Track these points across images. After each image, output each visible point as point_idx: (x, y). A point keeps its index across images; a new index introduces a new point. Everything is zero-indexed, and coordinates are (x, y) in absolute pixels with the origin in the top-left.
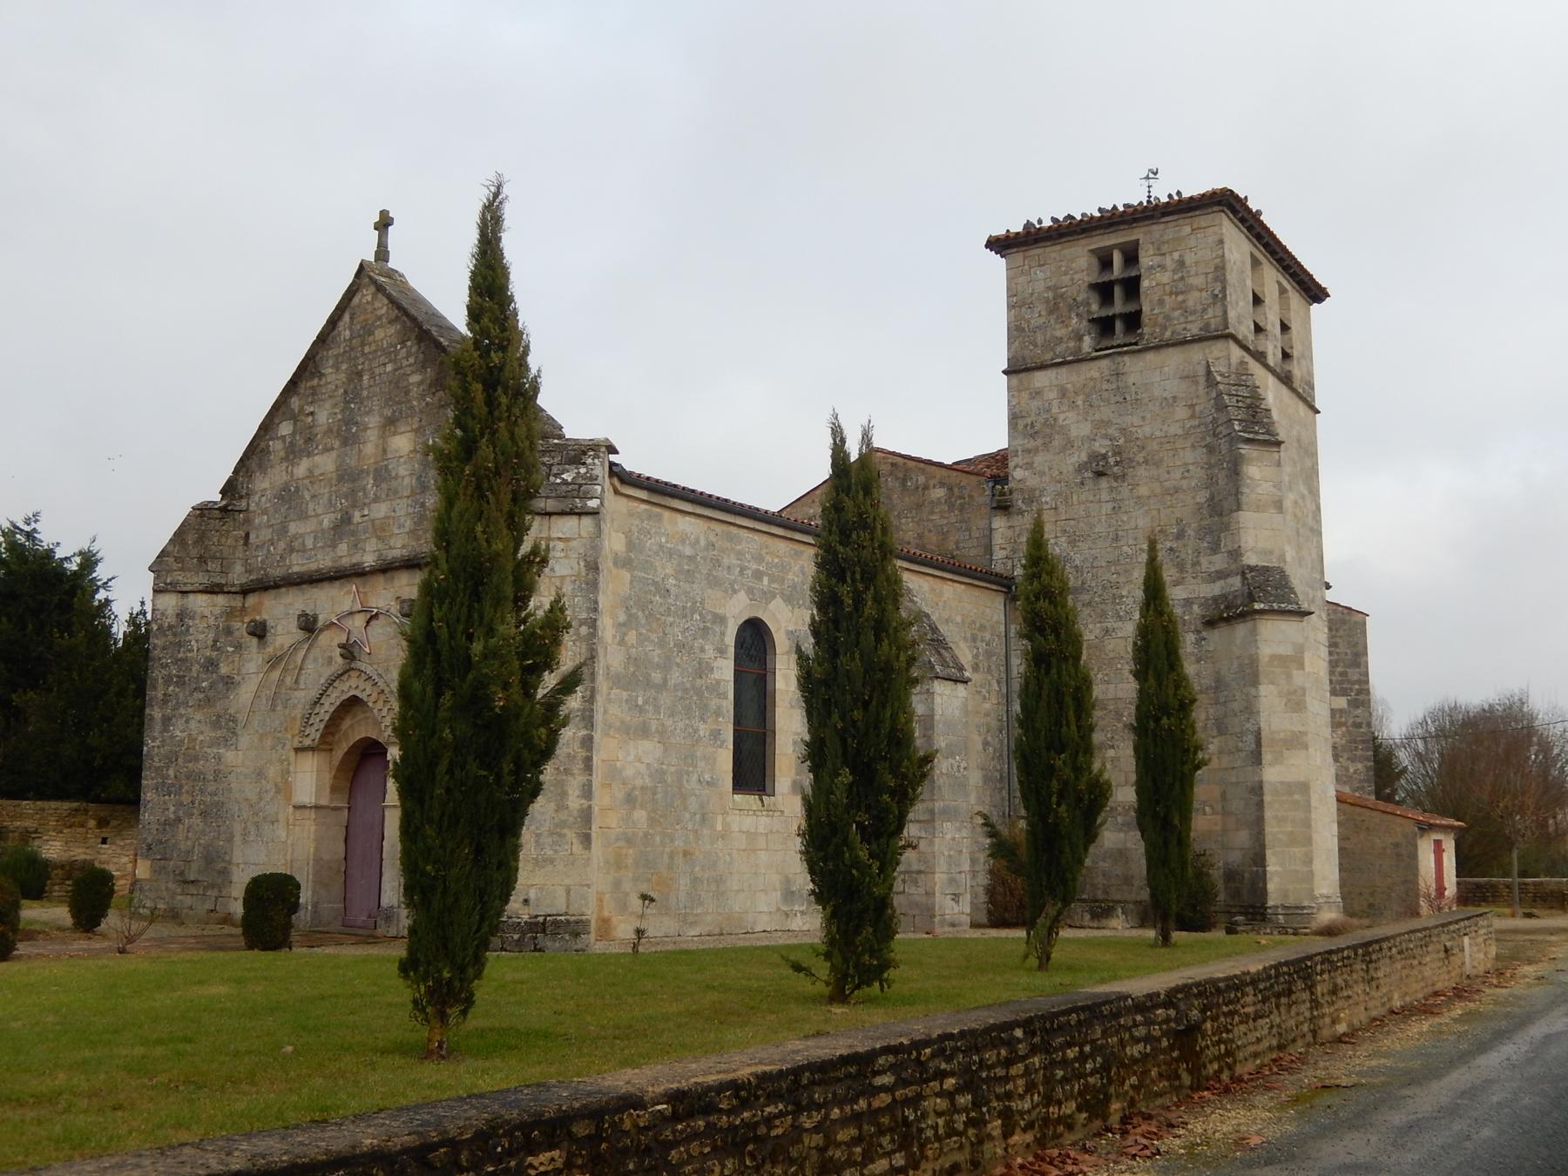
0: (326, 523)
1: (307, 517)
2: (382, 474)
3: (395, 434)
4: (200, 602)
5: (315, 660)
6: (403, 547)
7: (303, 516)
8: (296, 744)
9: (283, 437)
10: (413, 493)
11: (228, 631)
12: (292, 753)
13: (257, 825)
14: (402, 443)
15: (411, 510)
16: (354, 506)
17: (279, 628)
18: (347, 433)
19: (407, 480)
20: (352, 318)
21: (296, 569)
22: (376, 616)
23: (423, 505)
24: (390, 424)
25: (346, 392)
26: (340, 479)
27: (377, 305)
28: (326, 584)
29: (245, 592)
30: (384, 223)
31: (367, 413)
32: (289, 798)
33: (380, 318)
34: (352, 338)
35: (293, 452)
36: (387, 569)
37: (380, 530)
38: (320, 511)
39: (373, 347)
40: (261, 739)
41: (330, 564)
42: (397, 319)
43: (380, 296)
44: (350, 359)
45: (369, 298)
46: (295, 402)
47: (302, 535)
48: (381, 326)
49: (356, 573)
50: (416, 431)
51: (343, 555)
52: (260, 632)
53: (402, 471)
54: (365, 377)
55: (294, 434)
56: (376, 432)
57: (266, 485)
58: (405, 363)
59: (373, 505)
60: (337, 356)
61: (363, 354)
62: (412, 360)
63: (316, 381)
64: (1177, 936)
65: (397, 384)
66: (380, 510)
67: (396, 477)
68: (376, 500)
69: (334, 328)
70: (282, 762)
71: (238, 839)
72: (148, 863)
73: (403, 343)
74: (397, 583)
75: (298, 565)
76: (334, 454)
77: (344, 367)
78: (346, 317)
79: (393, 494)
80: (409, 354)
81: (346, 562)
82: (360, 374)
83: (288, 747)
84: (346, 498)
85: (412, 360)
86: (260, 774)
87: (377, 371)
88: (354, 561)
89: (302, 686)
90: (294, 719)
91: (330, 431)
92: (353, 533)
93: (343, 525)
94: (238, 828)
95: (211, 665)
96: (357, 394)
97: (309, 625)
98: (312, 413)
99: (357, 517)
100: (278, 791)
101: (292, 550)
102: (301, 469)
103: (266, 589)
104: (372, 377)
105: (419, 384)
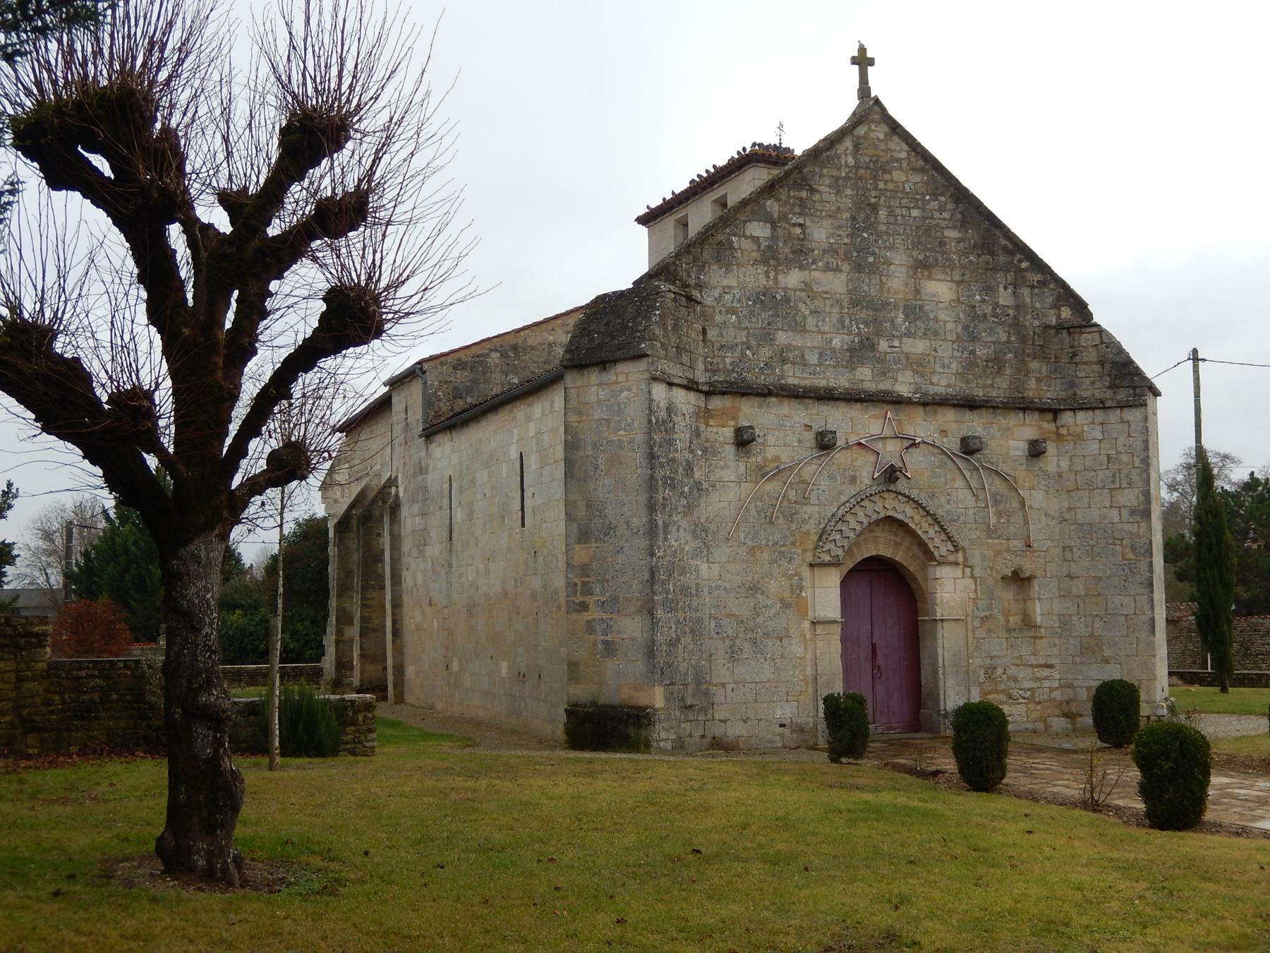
0: (836, 342)
1: (804, 331)
2: (915, 312)
3: (930, 278)
4: (680, 396)
5: (831, 477)
6: (949, 386)
7: (799, 327)
8: (809, 557)
9: (756, 240)
10: (958, 340)
11: (697, 433)
12: (806, 572)
13: (754, 643)
14: (940, 289)
15: (956, 354)
16: (879, 333)
17: (770, 437)
18: (861, 260)
19: (950, 326)
20: (857, 146)
21: (791, 381)
22: (914, 445)
23: (972, 352)
24: (922, 267)
25: (853, 218)
26: (855, 303)
27: (892, 145)
28: (842, 405)
29: (708, 394)
30: (863, 61)
31: (891, 248)
32: (803, 613)
33: (898, 160)
34: (857, 167)
35: (776, 259)
36: (932, 403)
37: (918, 365)
38: (827, 329)
39: (891, 186)
40: (752, 551)
41: (847, 385)
42: (922, 170)
43: (895, 138)
44: (855, 187)
45: (881, 136)
46: (772, 206)
47: (801, 349)
48: (901, 169)
49: (898, 402)
50: (959, 283)
51: (865, 377)
52: (743, 440)
53: (942, 315)
54: (883, 213)
55: (774, 238)
56: (904, 270)
57: (731, 281)
58: (937, 215)
59: (904, 340)
60: (837, 179)
61: (876, 188)
62: (946, 215)
63: (804, 194)
64: (1230, 689)
65: (928, 231)
66: (917, 346)
67: (936, 320)
68: (909, 334)
69: (828, 149)
70: (790, 577)
71: (720, 659)
72: (662, 689)
73: (935, 196)
74: (939, 417)
75: (793, 377)
76: (843, 277)
77: (849, 192)
78: (848, 143)
79: (932, 333)
80: (942, 211)
81: (871, 386)
82: (874, 208)
83: (798, 560)
84: (866, 323)
85: (946, 215)
86: (753, 589)
87: (898, 211)
88: (882, 387)
89: (814, 500)
90: (807, 533)
91: (831, 250)
92: (879, 361)
93: (862, 350)
94: (720, 649)
95: (689, 468)
96: (870, 226)
97: (825, 443)
98: (801, 225)
99: (883, 345)
100: (786, 606)
101: (784, 361)
102: (793, 279)
103: (743, 395)
104: (891, 213)
105: (959, 241)
